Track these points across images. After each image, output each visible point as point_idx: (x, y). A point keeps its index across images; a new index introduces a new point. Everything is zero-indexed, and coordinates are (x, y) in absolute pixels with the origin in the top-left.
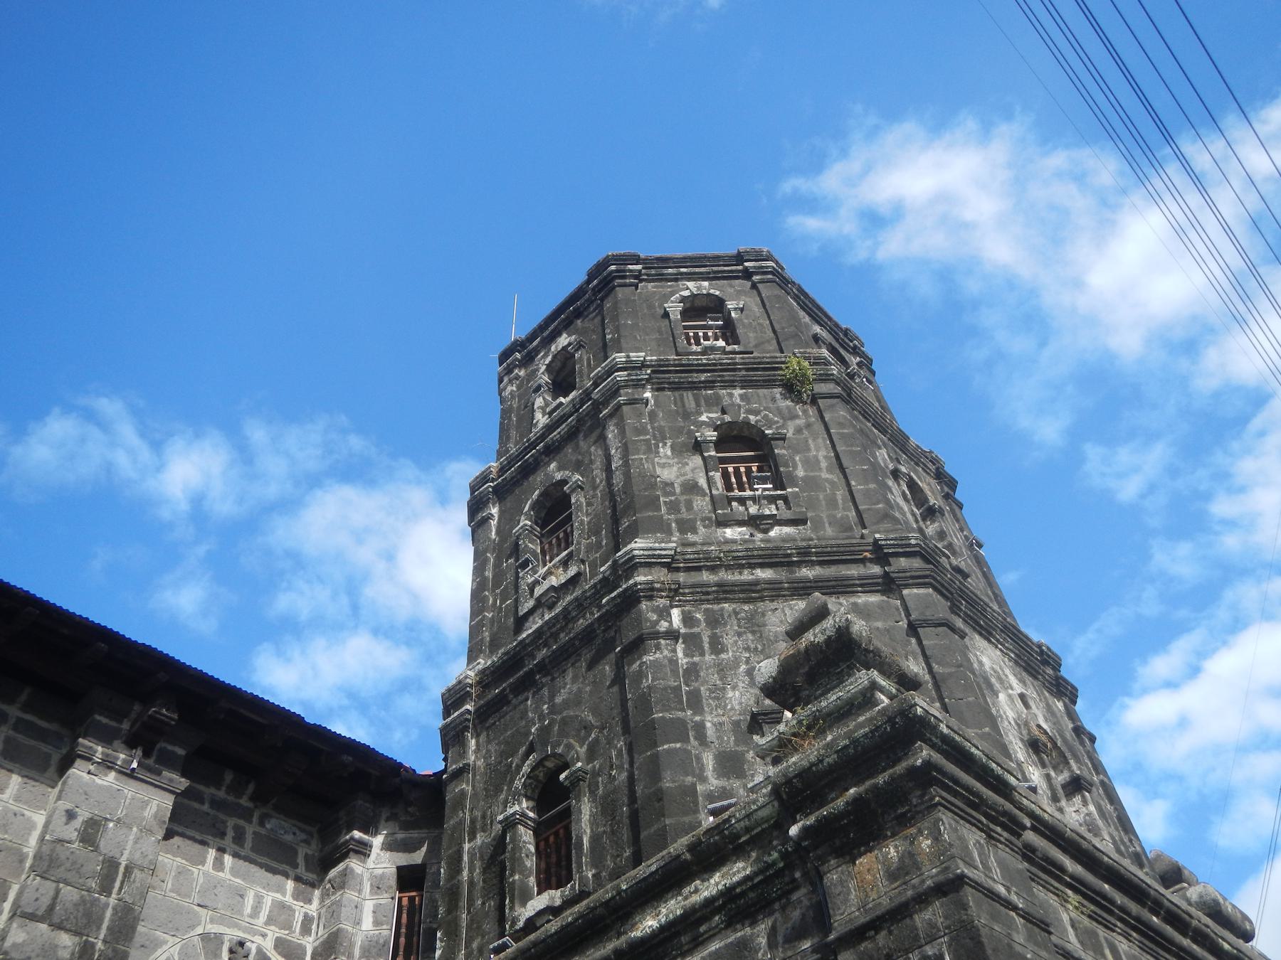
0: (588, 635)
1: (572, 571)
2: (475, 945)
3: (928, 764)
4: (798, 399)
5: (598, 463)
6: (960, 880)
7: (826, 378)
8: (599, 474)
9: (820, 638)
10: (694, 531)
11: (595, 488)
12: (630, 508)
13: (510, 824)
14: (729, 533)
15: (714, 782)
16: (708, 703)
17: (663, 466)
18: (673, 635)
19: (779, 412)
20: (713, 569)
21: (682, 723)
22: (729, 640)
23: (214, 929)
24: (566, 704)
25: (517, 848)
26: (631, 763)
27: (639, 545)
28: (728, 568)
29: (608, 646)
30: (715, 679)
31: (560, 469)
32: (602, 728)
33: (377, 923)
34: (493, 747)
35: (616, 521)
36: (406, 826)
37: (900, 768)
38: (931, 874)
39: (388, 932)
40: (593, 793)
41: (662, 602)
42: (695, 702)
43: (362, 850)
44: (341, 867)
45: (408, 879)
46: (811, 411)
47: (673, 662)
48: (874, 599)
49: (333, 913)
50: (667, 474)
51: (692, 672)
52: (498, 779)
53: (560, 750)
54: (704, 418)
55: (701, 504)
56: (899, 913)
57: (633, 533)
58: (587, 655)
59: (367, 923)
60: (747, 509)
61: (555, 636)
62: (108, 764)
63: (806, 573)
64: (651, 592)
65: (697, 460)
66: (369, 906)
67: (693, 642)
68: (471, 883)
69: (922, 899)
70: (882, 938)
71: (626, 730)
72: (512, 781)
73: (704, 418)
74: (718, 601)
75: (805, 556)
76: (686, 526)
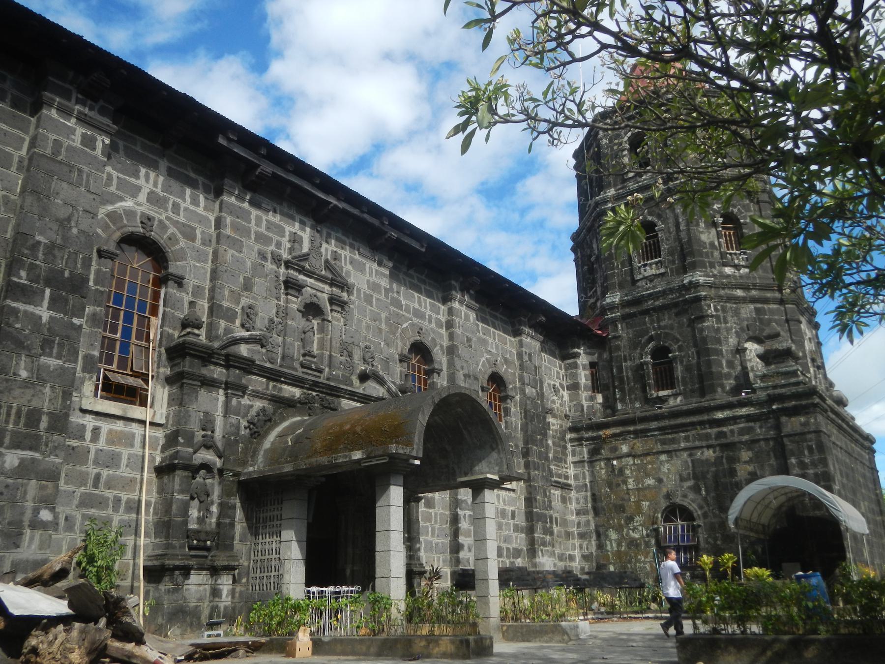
0: (675, 305)
1: (662, 270)
2: (633, 396)
3: (818, 403)
4: (752, 201)
5: (671, 221)
6: (821, 431)
7: (764, 191)
8: (673, 229)
9: (780, 348)
10: (715, 268)
11: (670, 233)
12: (692, 254)
13: (646, 363)
14: (728, 270)
15: (726, 370)
16: (724, 342)
17: (702, 232)
18: (712, 316)
19: (744, 206)
20: (723, 288)
21: (716, 350)
22: (729, 318)
23: (549, 381)
24: (665, 327)
25: (649, 372)
26: (699, 358)
27: (699, 277)
28: (729, 288)
29: (685, 311)
30: (725, 333)
31: (650, 214)
32: (684, 342)
33: (586, 380)
34: (630, 331)
35: (683, 256)
36: (589, 348)
37: (810, 401)
38: (813, 428)
39: (589, 383)
40: (682, 362)
41: (708, 302)
42: (718, 341)
43: (577, 355)
44: (572, 360)
45: (592, 365)
46: (757, 207)
47: (713, 326)
48: (775, 306)
49: (575, 376)
50: (704, 237)
51: (718, 330)
52: (635, 344)
53: (667, 344)
54: (715, 207)
55: (716, 254)
56: (803, 434)
57: (694, 266)
58: (674, 311)
59: (583, 380)
60: (732, 259)
61: (658, 298)
62: (528, 335)
63: (754, 293)
64: (705, 298)
65: (713, 231)
66: (583, 374)
67: (718, 318)
68: (627, 377)
69: (809, 432)
70: (797, 438)
71: (695, 345)
72: (643, 349)
73: (715, 207)
74: (726, 302)
75: (755, 287)
76: (712, 266)
